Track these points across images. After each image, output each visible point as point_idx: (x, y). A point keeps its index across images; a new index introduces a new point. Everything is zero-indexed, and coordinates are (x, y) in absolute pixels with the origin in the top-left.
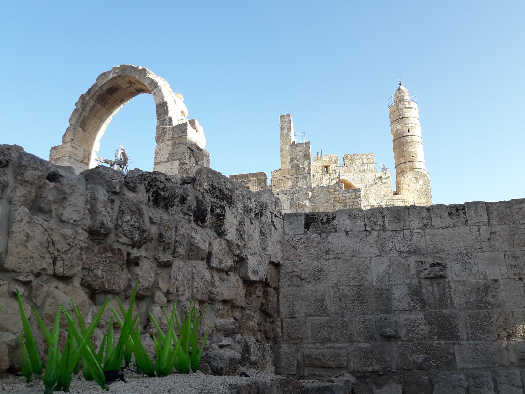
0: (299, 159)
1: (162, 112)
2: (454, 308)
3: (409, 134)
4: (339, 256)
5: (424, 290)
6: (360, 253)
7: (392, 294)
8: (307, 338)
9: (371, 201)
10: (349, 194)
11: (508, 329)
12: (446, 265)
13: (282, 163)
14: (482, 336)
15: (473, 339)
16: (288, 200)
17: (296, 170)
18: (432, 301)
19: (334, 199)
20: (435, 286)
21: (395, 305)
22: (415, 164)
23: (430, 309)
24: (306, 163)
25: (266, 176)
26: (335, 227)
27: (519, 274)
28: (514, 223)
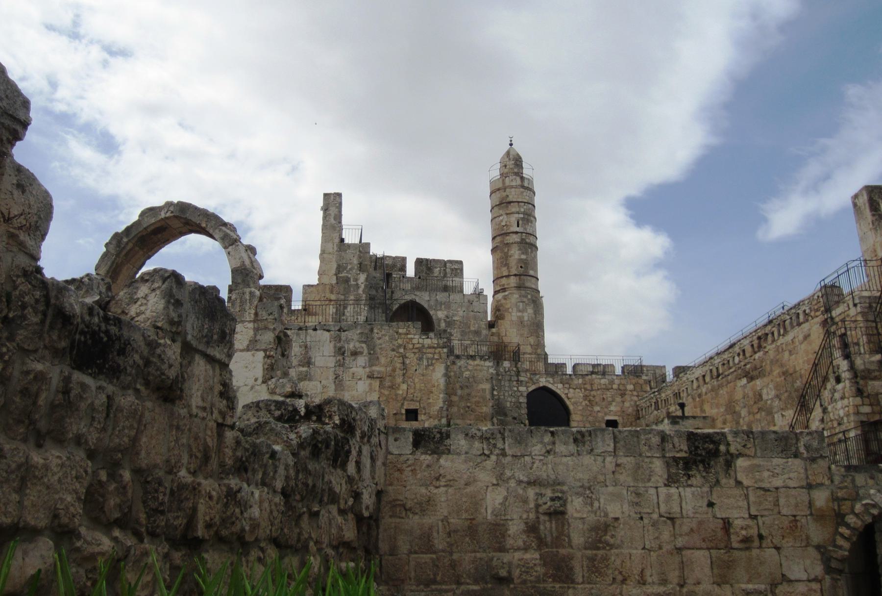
0: (351, 269)
2: (572, 547)
3: (518, 229)
4: (452, 483)
5: (542, 527)
6: (475, 481)
7: (507, 530)
8: (410, 579)
11: (624, 573)
12: (567, 499)
14: (598, 579)
15: (589, 583)
17: (345, 288)
18: (549, 539)
20: (554, 522)
21: (510, 542)
23: (547, 548)
27: (640, 513)
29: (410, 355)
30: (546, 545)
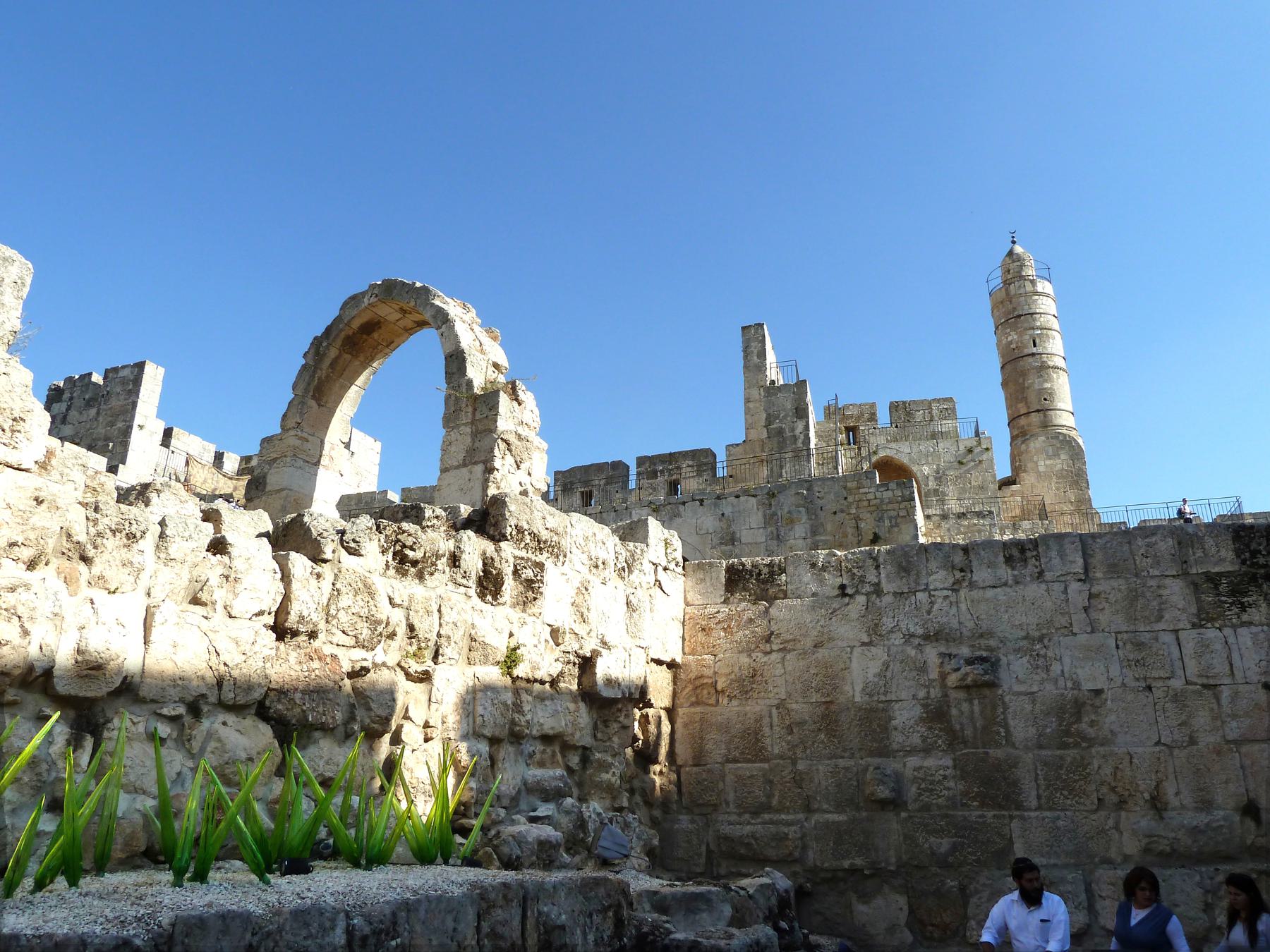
0: (785, 417)
1: (455, 370)
2: (1013, 746)
3: (1034, 350)
4: (789, 646)
5: (954, 712)
6: (830, 639)
7: (891, 719)
8: (727, 804)
9: (951, 502)
10: (889, 494)
11: (1119, 789)
12: (998, 660)
13: (748, 428)
14: (1069, 802)
15: (1050, 809)
16: (758, 509)
17: (779, 442)
18: (969, 732)
19: (858, 505)
20: (976, 702)
21: (897, 739)
22: (1051, 416)
23: (966, 747)
24: (800, 426)
25: (714, 456)
26: (784, 588)
28: (1137, 575)
29: (865, 515)
30: (965, 743)
